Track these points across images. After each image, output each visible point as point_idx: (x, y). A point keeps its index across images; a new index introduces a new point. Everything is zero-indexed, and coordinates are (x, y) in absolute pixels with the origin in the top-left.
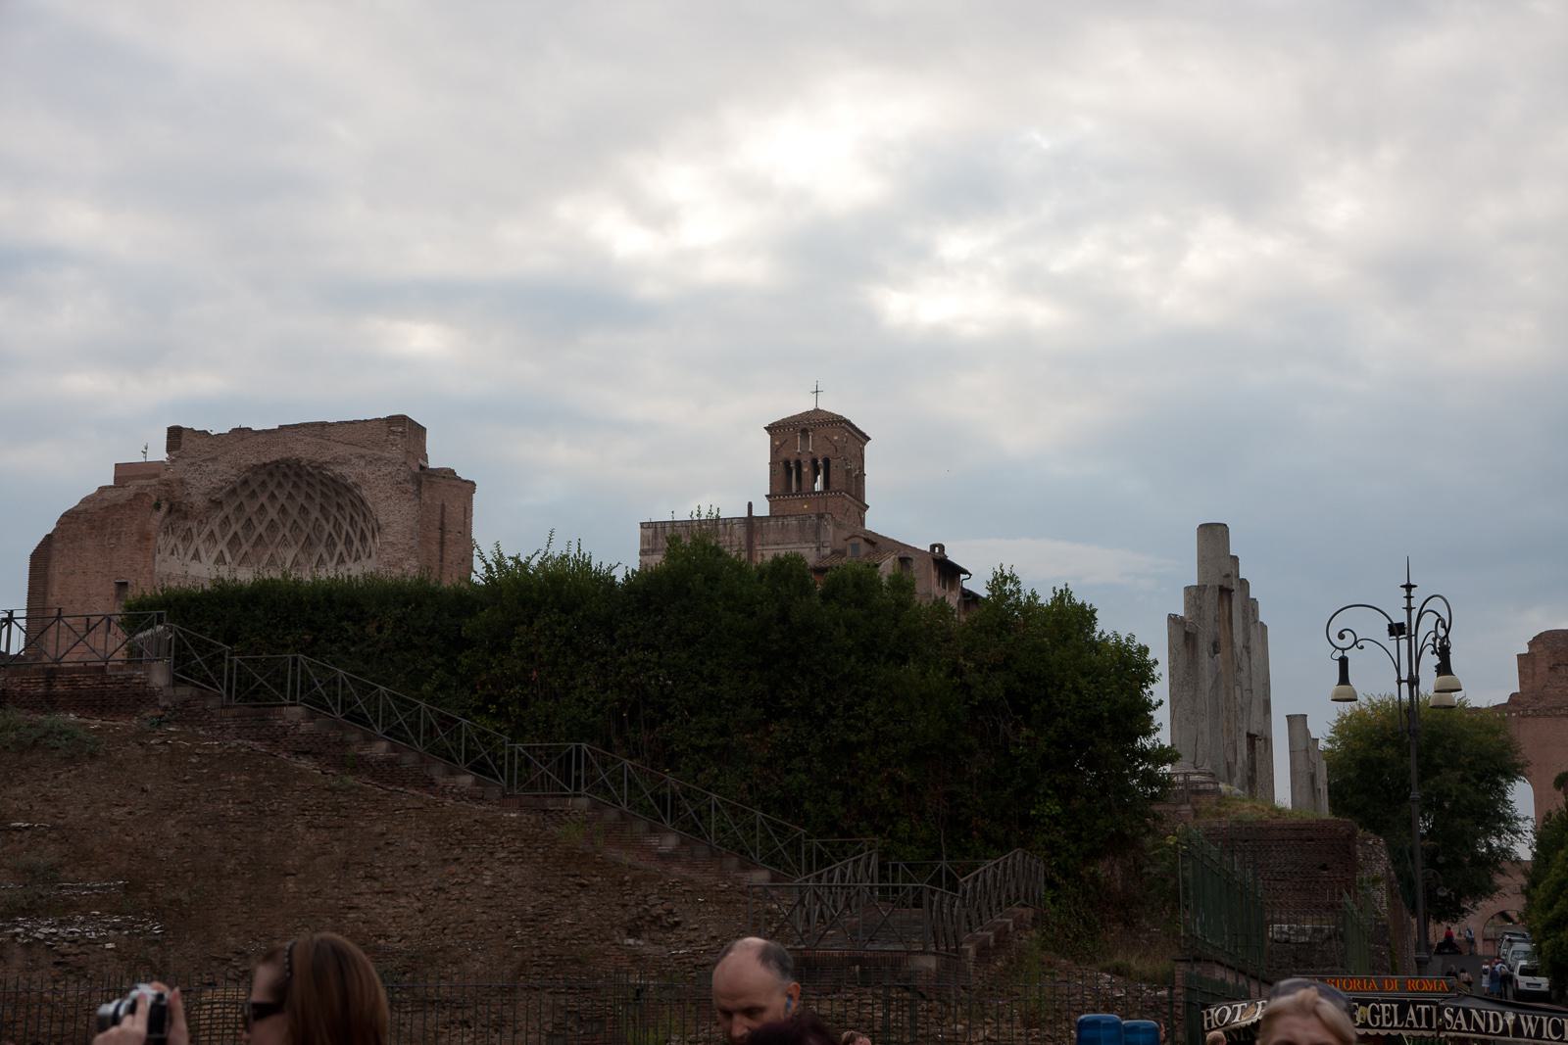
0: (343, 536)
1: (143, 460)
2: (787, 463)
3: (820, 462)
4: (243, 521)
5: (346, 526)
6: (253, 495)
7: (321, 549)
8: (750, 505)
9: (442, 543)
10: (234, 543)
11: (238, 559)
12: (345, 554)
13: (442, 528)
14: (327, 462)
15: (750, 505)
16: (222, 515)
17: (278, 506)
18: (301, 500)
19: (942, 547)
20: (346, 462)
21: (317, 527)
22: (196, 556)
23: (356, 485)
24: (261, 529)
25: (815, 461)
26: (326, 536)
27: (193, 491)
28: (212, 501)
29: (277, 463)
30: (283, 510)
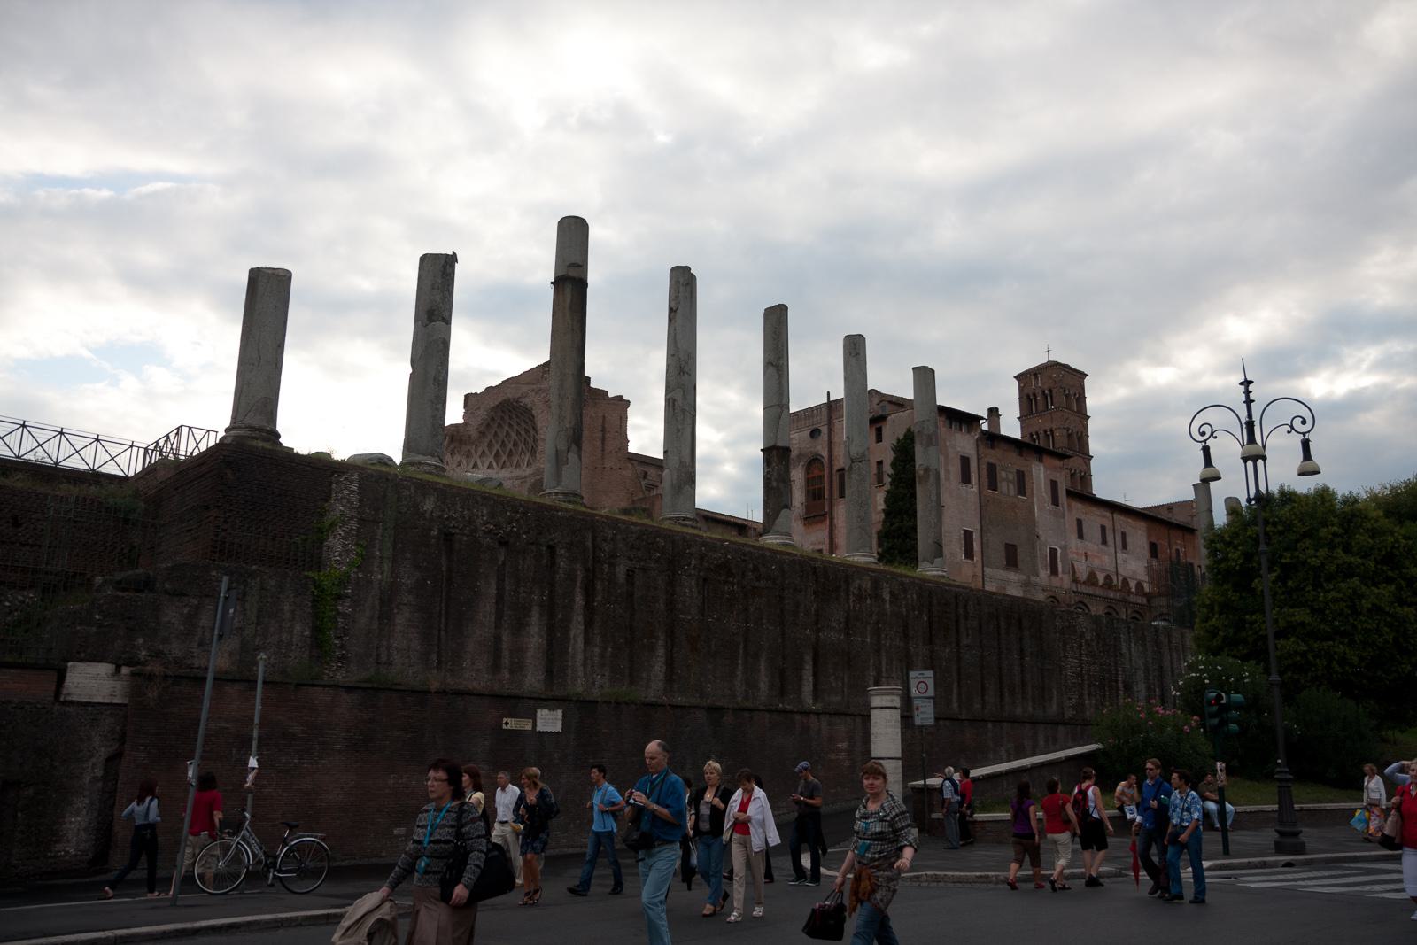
2: (1028, 396)
3: (1046, 392)
4: (500, 443)
6: (500, 425)
8: (828, 393)
9: (603, 440)
10: (497, 456)
11: (500, 465)
13: (603, 430)
14: (519, 398)
15: (828, 393)
20: (525, 395)
22: (475, 466)
24: (510, 446)
27: (471, 428)
28: (480, 432)
30: (518, 433)
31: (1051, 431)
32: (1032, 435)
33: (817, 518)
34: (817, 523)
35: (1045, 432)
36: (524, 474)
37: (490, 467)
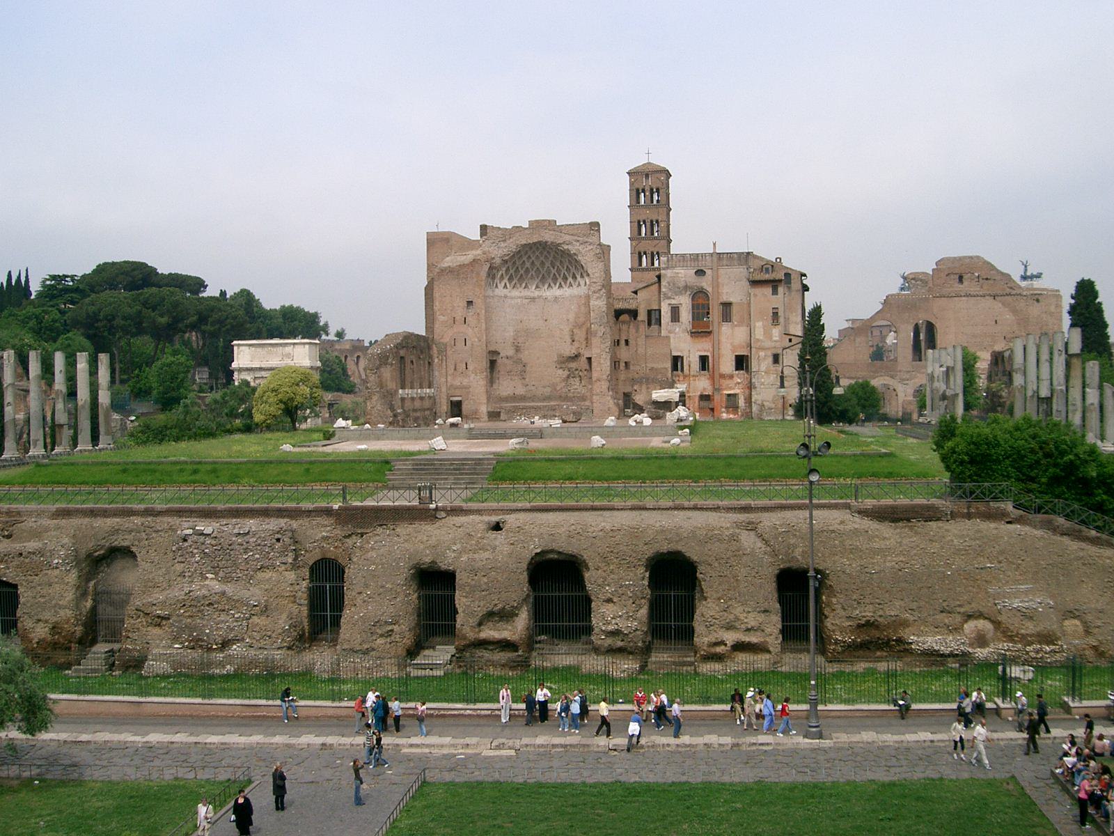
0: (562, 275)
1: (436, 231)
5: (564, 271)
6: (521, 256)
7: (550, 281)
10: (510, 279)
12: (563, 283)
16: (507, 266)
17: (531, 261)
18: (542, 258)
19: (780, 259)
21: (549, 272)
23: (575, 254)
24: (522, 272)
25: (652, 190)
26: (552, 275)
29: (535, 244)
31: (657, 222)
32: (639, 222)
33: (702, 334)
34: (702, 337)
35: (652, 221)
36: (532, 295)
37: (505, 286)
